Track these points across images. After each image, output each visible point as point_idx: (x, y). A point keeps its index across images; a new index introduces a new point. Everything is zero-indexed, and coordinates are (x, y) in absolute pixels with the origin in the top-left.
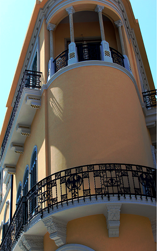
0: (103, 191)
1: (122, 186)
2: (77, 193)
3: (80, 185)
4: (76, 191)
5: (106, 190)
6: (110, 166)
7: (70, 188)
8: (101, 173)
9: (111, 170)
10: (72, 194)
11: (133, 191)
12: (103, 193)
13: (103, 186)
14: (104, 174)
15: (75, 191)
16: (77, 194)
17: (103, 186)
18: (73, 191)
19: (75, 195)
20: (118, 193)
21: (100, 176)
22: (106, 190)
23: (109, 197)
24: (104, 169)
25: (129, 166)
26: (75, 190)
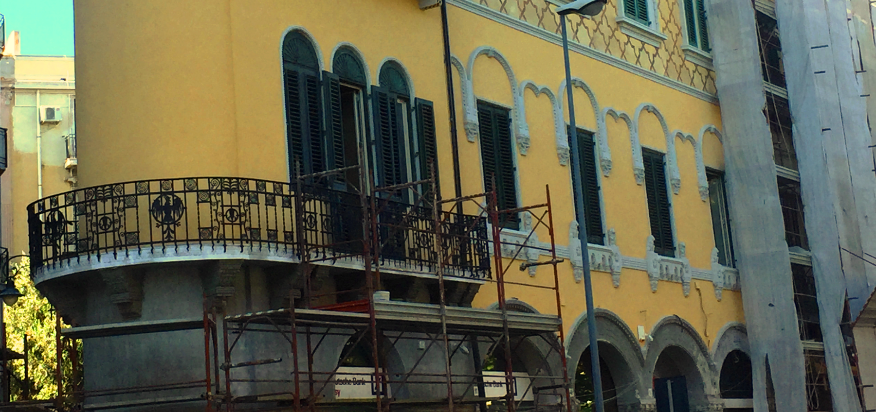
0: (215, 233)
1: (247, 225)
2: (174, 232)
3: (180, 217)
4: (172, 227)
5: (221, 231)
6: (230, 183)
7: (160, 219)
8: (213, 197)
9: (230, 191)
10: (164, 233)
11: (264, 235)
12: (215, 237)
13: (215, 224)
14: (219, 198)
15: (169, 228)
16: (172, 235)
17: (215, 224)
18: (165, 227)
19: (169, 236)
20: (241, 240)
21: (210, 202)
22: (221, 231)
23: (225, 246)
24: (219, 188)
25: (261, 184)
26: (168, 225)
